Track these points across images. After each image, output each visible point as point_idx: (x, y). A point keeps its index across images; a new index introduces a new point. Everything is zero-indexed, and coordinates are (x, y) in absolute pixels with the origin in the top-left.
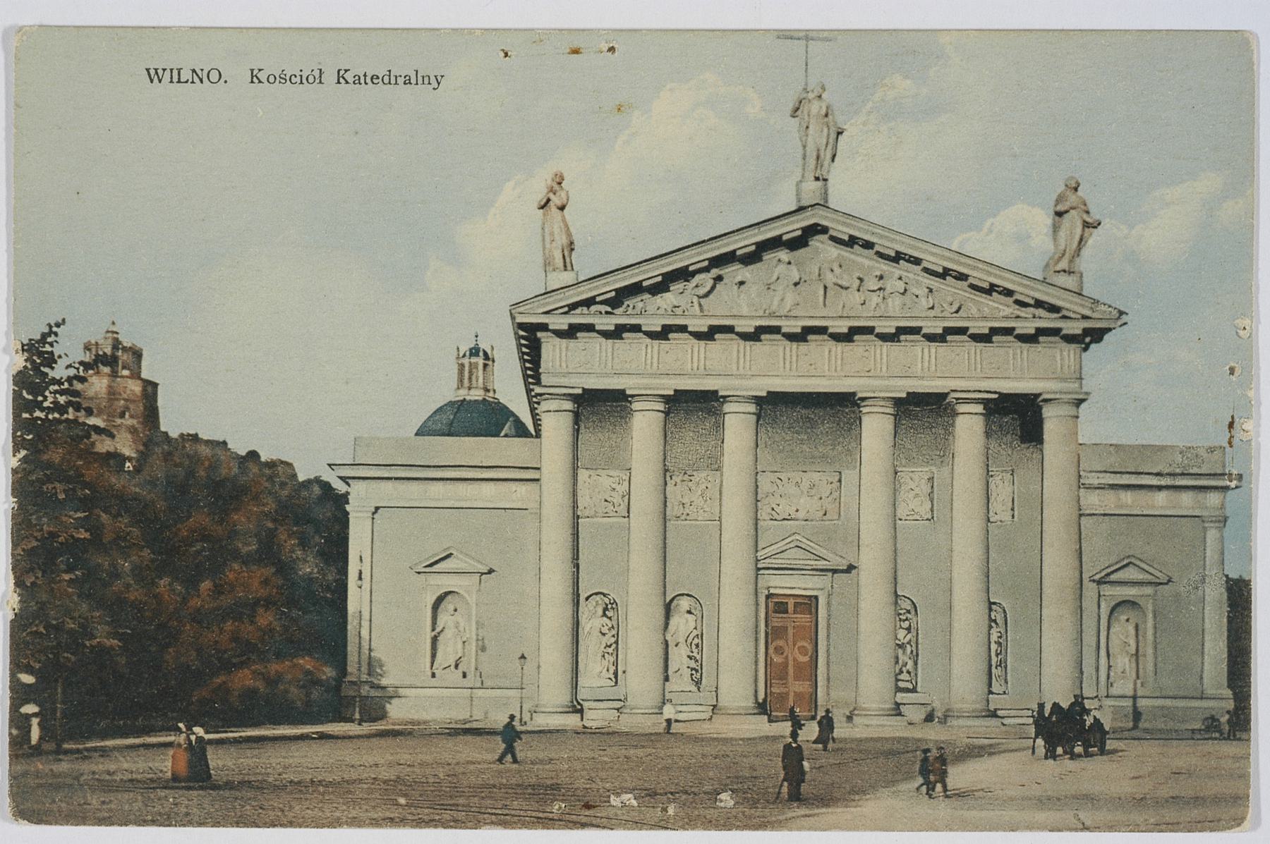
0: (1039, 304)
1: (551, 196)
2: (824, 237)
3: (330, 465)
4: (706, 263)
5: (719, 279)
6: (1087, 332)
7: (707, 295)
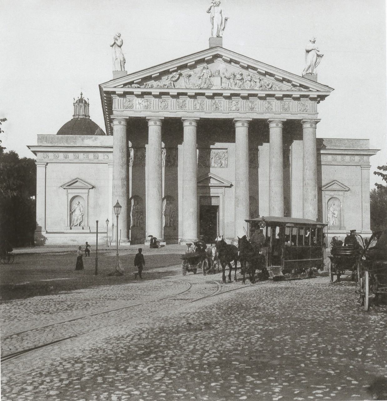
0: (301, 86)
1: (116, 41)
2: (221, 59)
3: (28, 147)
4: (176, 68)
5: (180, 75)
6: (319, 96)
7: (176, 81)
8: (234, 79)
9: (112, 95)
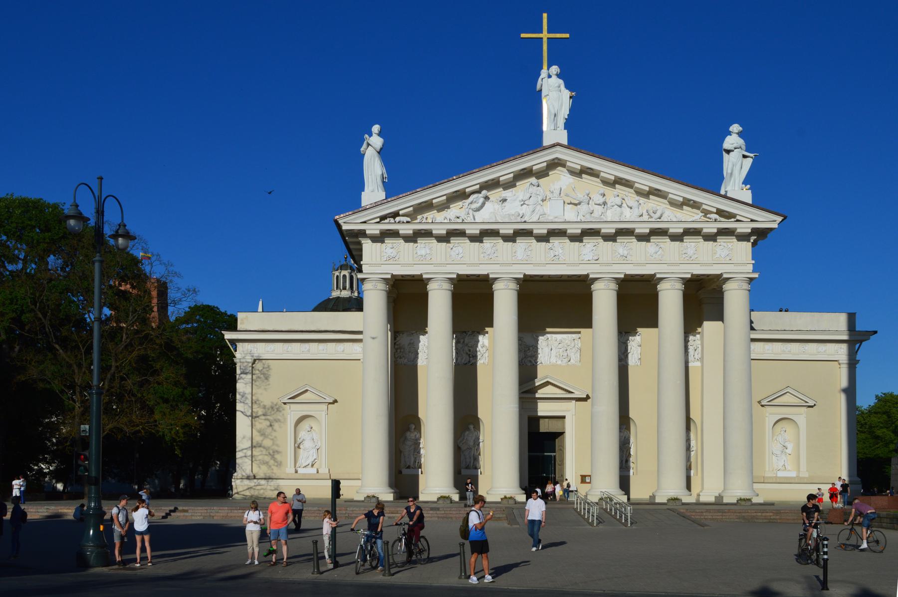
0: (720, 212)
4: (478, 186)
5: (487, 198)
7: (478, 210)
8: (588, 204)
9: (360, 239)
